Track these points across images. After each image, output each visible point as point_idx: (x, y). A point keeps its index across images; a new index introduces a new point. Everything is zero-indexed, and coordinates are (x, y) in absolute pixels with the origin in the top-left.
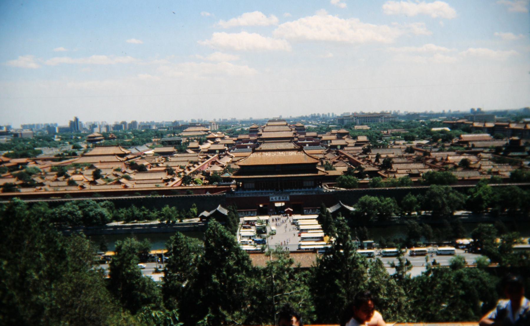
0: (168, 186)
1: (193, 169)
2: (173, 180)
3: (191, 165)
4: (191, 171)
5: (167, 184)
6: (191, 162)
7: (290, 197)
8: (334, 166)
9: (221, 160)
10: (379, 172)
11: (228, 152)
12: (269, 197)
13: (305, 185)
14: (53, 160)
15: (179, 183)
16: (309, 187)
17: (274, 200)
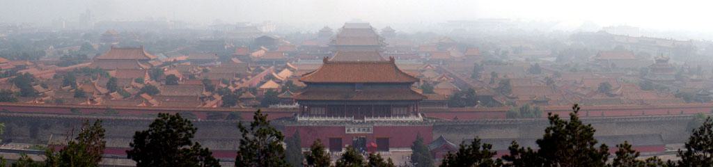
0: (205, 106)
1: (239, 85)
2: (211, 98)
3: (238, 79)
4: (237, 88)
5: (205, 104)
6: (237, 75)
7: (375, 128)
8: (435, 87)
9: (280, 74)
10: (494, 98)
11: (288, 64)
12: (344, 128)
13: (395, 112)
14: (59, 65)
15: (221, 103)
16: (401, 116)
17: (352, 132)
